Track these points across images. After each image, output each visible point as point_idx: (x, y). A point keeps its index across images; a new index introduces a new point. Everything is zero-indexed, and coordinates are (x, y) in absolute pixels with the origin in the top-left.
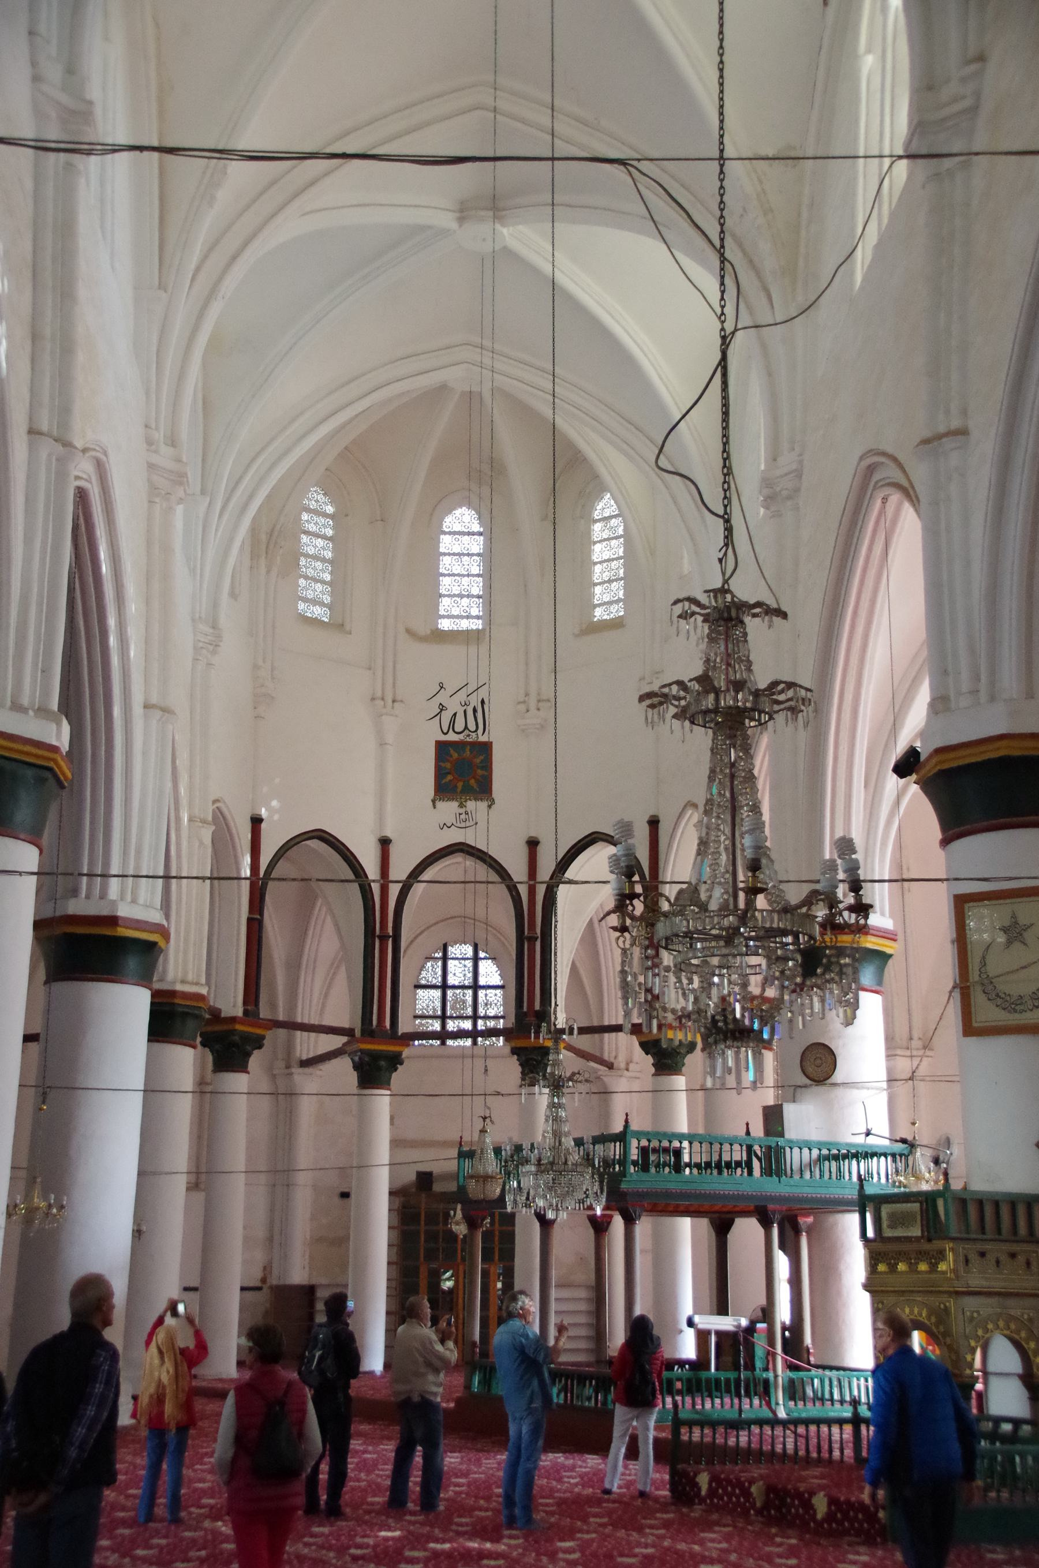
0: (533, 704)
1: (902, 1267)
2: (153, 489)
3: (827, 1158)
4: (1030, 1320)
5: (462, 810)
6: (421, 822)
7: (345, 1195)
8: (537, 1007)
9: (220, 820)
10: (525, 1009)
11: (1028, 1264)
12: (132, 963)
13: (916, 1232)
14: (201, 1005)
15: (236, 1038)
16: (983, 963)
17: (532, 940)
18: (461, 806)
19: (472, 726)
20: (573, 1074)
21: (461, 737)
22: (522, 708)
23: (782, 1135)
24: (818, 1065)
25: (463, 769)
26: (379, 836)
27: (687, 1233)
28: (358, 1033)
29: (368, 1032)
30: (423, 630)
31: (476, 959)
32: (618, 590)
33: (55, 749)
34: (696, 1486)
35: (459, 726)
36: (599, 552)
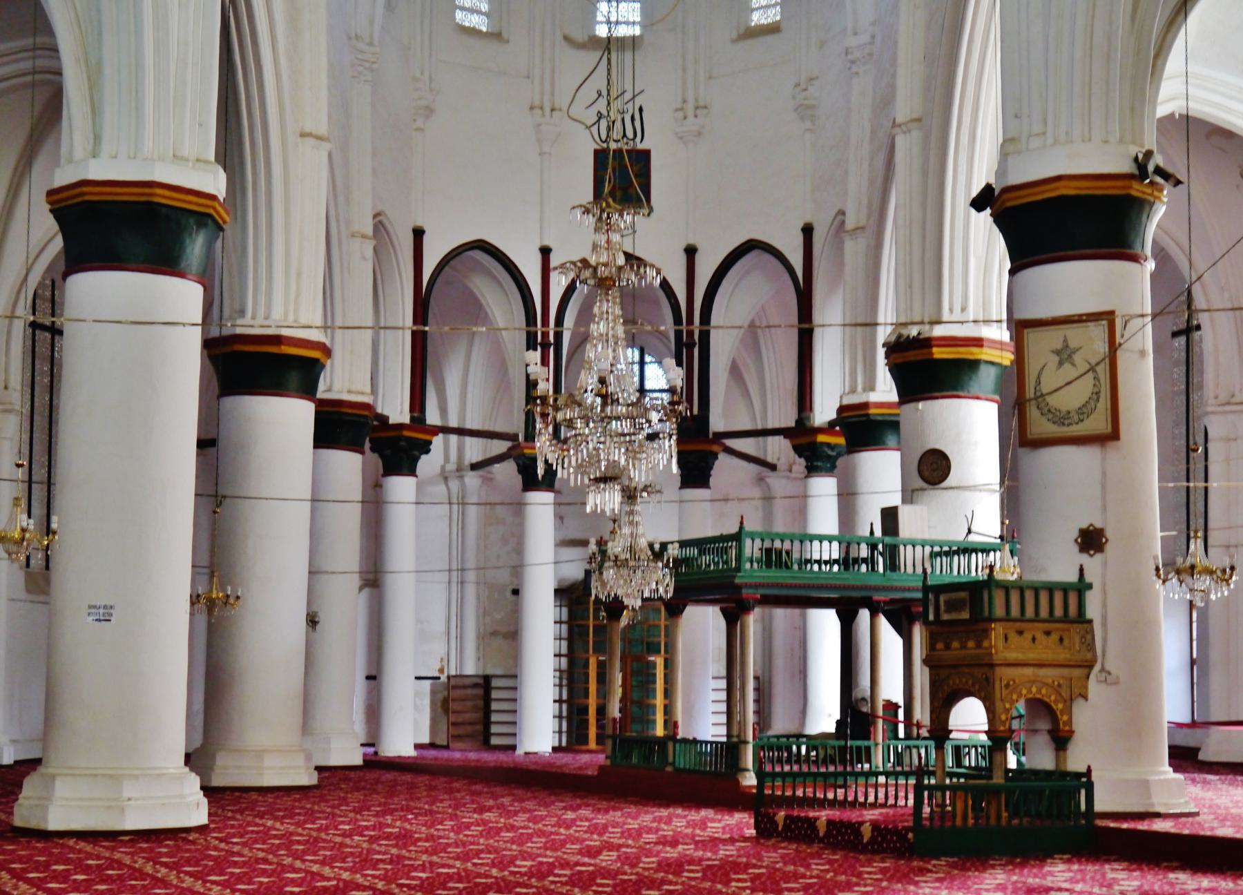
0: (690, 113)
1: (955, 645)
3: (939, 554)
4: (1059, 685)
7: (516, 592)
11: (1061, 640)
12: (294, 378)
13: (965, 615)
14: (366, 413)
15: (403, 443)
16: (1038, 383)
17: (690, 346)
19: (630, 134)
20: (646, 487)
22: (680, 114)
24: (933, 468)
25: (623, 179)
26: (538, 246)
27: (825, 626)
28: (521, 438)
30: (580, 36)
31: (642, 363)
33: (213, 197)
34: (775, 824)
35: (617, 134)
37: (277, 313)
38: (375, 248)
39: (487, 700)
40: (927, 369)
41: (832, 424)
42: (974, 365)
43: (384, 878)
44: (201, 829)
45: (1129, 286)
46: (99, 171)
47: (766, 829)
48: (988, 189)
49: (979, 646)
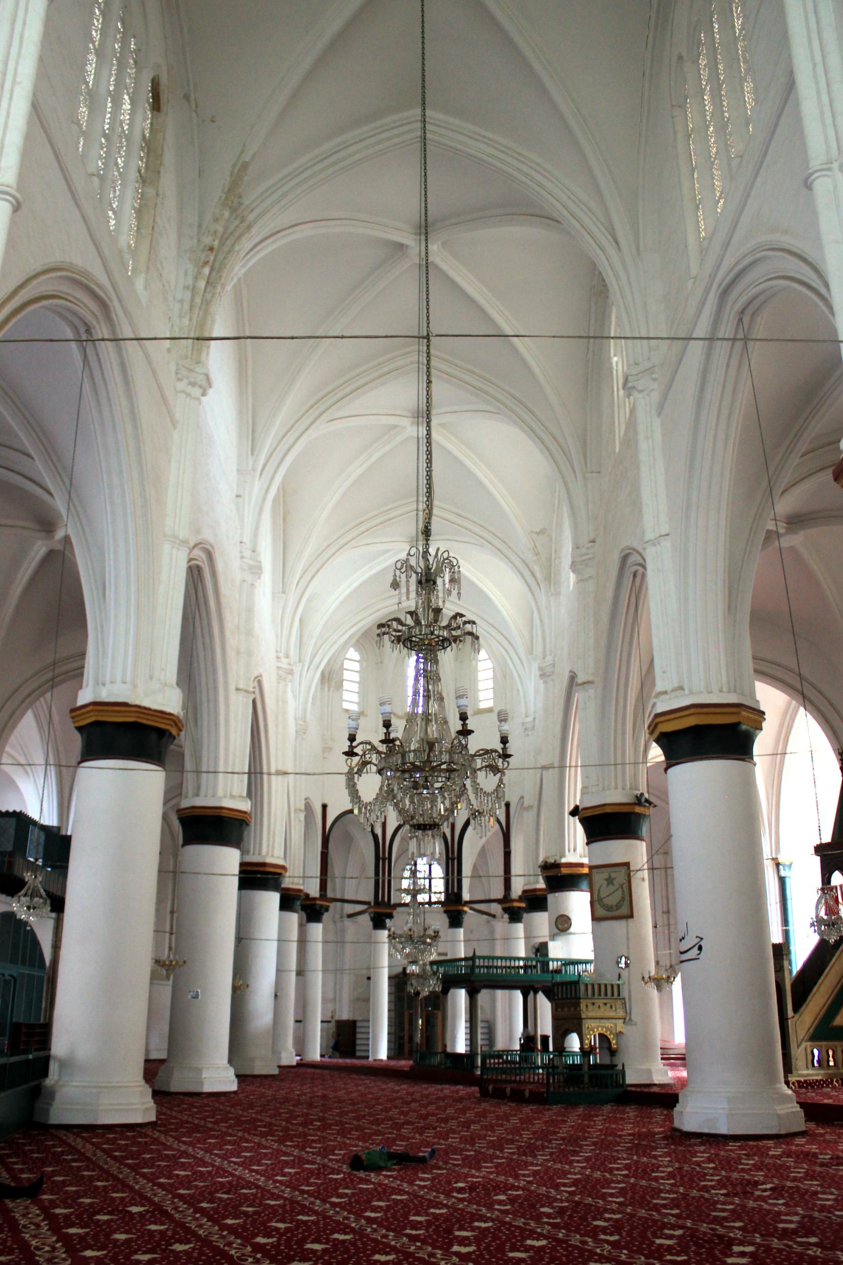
1: (566, 1009)
2: (280, 677)
7: (369, 978)
8: (456, 890)
9: (308, 808)
11: (611, 1007)
17: (453, 859)
23: (547, 955)
24: (562, 925)
27: (518, 995)
32: (490, 694)
33: (245, 812)
36: (481, 676)
37: (264, 852)
38: (306, 817)
39: (354, 1034)
40: (560, 878)
41: (520, 897)
42: (580, 876)
43: (321, 1111)
44: (235, 1092)
45: (636, 852)
46: (200, 802)
47: (484, 1094)
48: (577, 808)
49: (576, 1009)
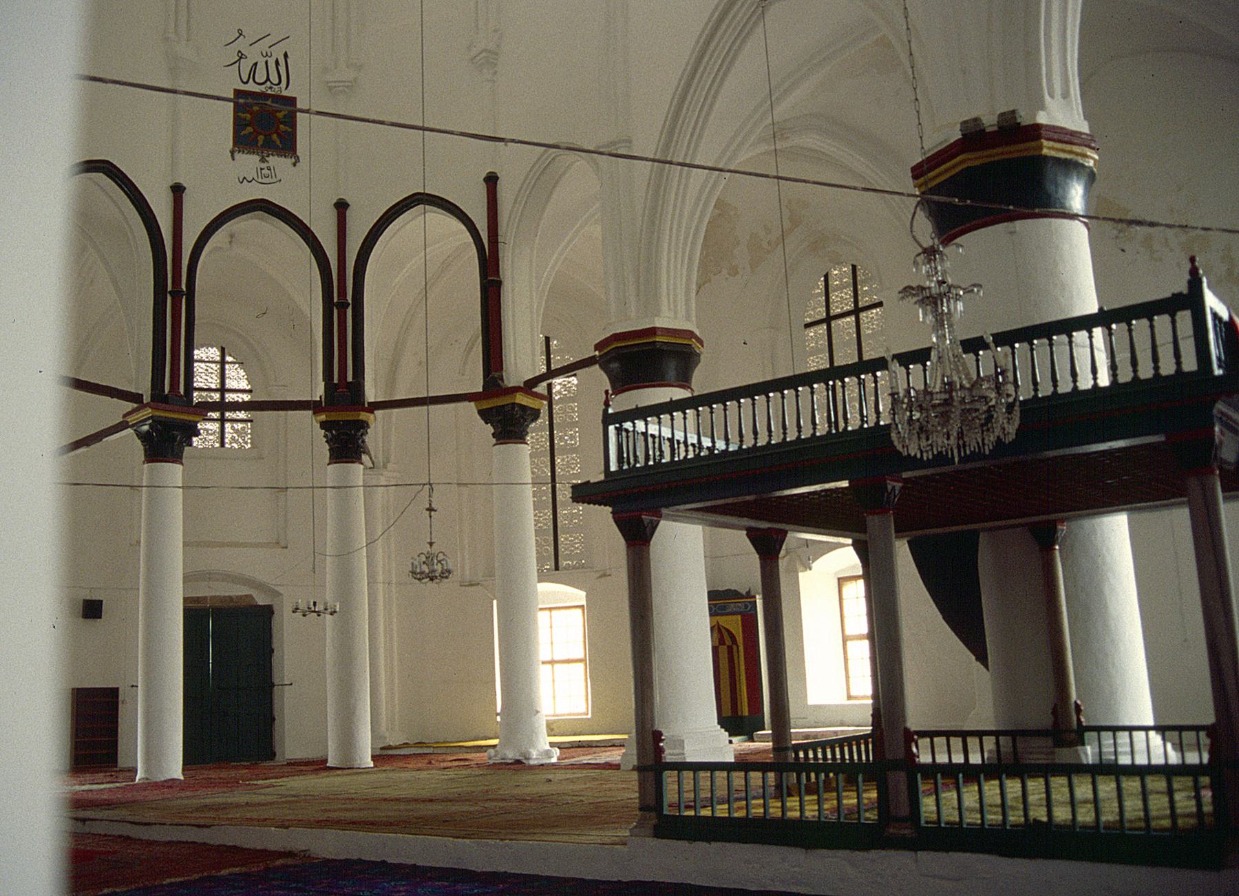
5: (263, 165)
6: (220, 174)
8: (350, 379)
10: (336, 381)
17: (343, 306)
18: (263, 160)
19: (275, 79)
21: (262, 88)
28: (147, 399)
29: (158, 396)
31: (223, 362)
35: (261, 77)
